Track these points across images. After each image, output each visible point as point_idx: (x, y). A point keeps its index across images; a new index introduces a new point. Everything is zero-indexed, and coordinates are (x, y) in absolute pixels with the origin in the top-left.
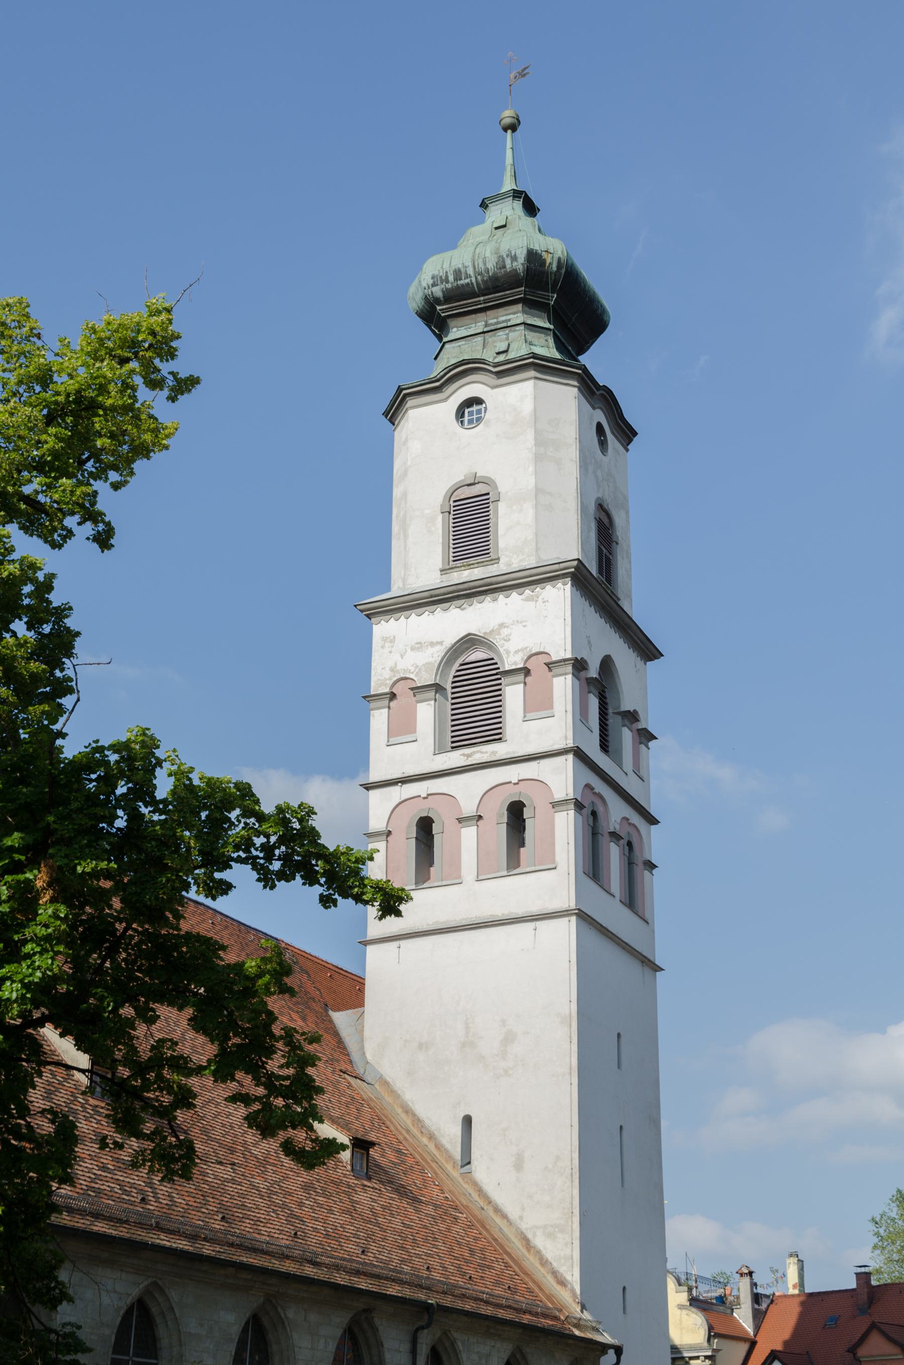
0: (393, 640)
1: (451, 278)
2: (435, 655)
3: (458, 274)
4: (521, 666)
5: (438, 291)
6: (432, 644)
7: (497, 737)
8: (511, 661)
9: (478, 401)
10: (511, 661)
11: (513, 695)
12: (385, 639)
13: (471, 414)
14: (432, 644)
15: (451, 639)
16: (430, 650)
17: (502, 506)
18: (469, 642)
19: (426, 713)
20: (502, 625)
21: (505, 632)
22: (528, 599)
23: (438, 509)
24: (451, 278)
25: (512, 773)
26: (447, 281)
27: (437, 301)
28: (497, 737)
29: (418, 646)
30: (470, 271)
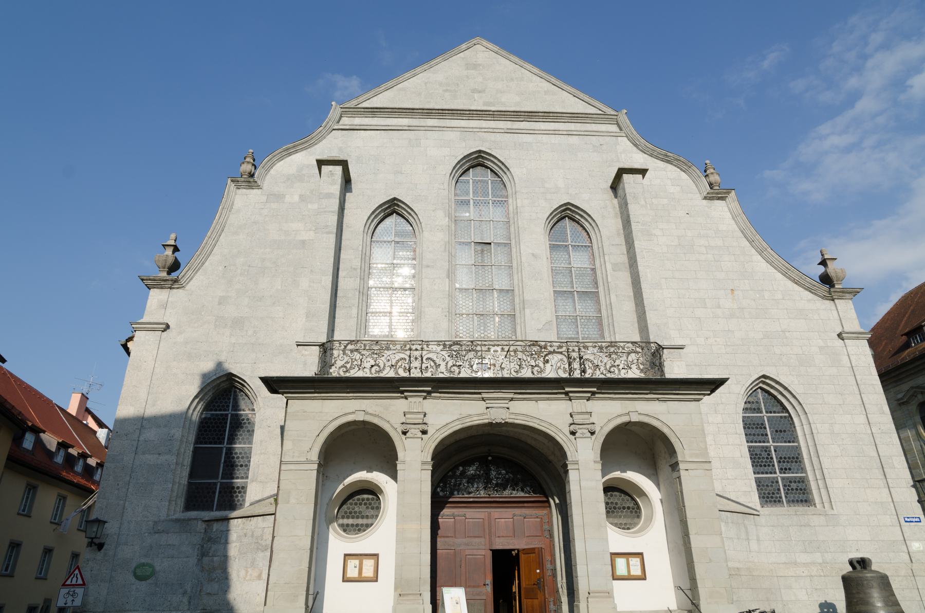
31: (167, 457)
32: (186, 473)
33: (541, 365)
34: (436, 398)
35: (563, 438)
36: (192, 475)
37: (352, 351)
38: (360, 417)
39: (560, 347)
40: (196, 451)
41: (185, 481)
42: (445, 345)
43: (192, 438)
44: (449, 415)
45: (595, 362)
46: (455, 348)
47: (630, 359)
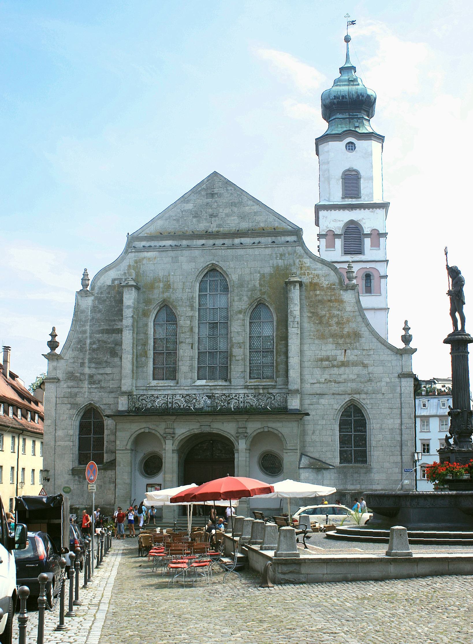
0: (326, 218)
1: (341, 98)
2: (341, 224)
3: (343, 97)
4: (369, 233)
5: (335, 101)
6: (339, 221)
7: (360, 252)
8: (367, 231)
9: (352, 143)
10: (367, 231)
11: (367, 242)
12: (324, 217)
13: (349, 146)
14: (339, 221)
15: (347, 220)
16: (339, 223)
17: (362, 180)
18: (352, 222)
19: (339, 243)
20: (363, 218)
21: (364, 221)
22: (371, 212)
23: (340, 177)
24: (341, 98)
25: (368, 265)
26: (339, 98)
27: (334, 104)
28: (360, 252)
29: (335, 221)
30: (347, 97)
31: (68, 443)
32: (77, 449)
33: (226, 405)
34: (178, 421)
35: (232, 439)
36: (79, 450)
37: (142, 400)
38: (147, 431)
39: (236, 396)
40: (79, 438)
41: (77, 452)
42: (183, 397)
43: (77, 433)
44: (183, 429)
45: (251, 403)
46: (188, 397)
47: (267, 402)
